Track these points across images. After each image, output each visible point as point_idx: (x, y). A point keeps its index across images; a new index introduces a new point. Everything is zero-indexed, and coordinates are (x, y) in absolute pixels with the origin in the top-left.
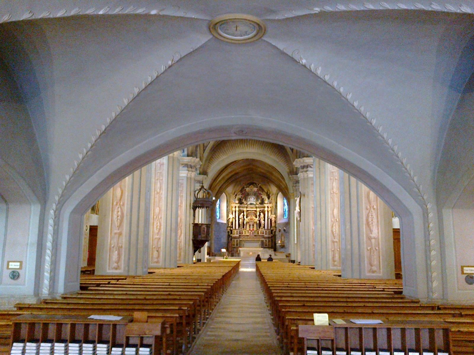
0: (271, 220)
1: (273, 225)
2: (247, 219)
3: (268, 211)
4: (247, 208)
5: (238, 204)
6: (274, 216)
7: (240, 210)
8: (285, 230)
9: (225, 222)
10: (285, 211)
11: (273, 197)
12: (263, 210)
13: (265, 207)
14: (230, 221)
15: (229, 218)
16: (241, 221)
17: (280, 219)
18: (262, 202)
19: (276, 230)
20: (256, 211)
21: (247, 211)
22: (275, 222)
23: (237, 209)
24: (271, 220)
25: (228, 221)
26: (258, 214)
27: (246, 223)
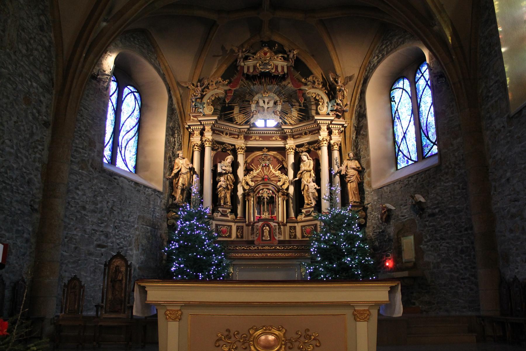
0: (343, 178)
1: (352, 198)
2: (248, 178)
3: (330, 148)
5: (214, 114)
6: (354, 164)
7: (222, 143)
8: (419, 208)
9: (160, 188)
10: (399, 140)
11: (346, 96)
12: (309, 143)
13: (318, 130)
14: (180, 184)
16: (222, 182)
17: (382, 173)
18: (306, 114)
19: (366, 218)
20: (282, 150)
21: (249, 150)
23: (208, 135)
24: (343, 178)
25: (171, 183)
26: (291, 159)
27: (244, 195)
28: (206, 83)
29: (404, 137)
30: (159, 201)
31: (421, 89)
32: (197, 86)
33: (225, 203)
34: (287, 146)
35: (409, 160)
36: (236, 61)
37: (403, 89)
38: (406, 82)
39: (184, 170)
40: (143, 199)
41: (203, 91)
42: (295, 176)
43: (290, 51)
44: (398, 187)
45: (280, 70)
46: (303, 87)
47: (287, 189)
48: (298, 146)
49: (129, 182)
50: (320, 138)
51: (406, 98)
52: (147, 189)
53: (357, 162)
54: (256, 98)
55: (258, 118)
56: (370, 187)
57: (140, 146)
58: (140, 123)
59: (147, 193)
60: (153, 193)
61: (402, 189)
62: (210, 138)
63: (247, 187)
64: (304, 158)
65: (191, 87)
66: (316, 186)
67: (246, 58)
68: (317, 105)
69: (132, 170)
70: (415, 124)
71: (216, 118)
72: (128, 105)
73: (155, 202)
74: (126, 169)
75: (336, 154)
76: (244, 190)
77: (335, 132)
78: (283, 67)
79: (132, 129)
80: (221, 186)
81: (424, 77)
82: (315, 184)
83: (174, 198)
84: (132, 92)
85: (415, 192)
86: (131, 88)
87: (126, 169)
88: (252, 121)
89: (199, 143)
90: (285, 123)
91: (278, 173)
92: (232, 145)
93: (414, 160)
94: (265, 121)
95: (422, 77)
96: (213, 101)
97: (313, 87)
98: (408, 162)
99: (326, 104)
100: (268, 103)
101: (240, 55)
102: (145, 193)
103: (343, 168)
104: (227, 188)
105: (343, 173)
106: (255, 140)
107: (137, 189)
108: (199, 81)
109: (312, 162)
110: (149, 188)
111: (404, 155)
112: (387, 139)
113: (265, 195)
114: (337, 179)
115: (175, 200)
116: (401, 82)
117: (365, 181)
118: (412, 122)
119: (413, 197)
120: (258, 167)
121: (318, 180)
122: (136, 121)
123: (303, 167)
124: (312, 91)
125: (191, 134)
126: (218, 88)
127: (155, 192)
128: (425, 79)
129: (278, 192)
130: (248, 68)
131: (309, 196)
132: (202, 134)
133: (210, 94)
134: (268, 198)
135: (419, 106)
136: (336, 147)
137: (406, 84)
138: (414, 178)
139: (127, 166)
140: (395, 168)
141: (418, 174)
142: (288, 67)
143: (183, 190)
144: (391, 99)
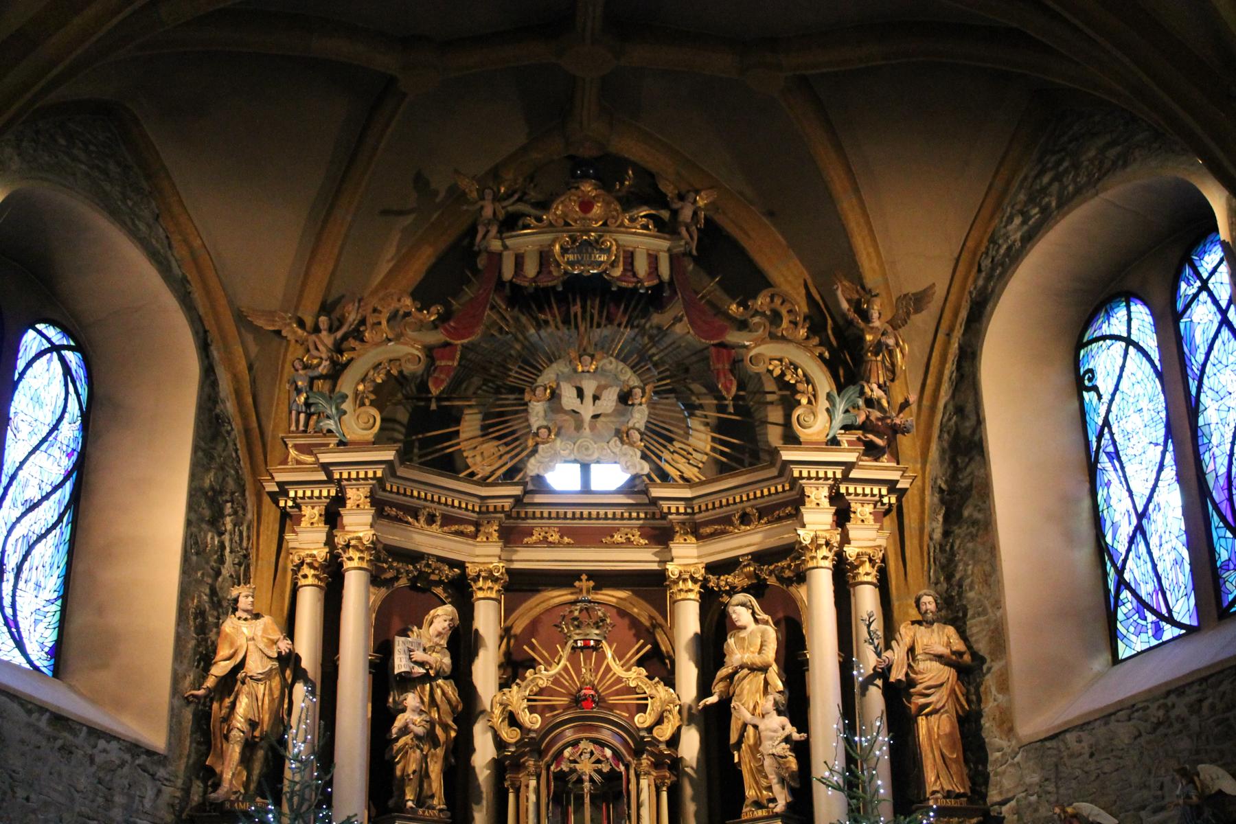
2: (516, 697)
4: (511, 536)
5: (379, 441)
6: (941, 639)
7: (415, 557)
9: (157, 739)
10: (1118, 540)
11: (904, 372)
12: (760, 557)
13: (794, 505)
14: (239, 721)
15: (220, 668)
16: (412, 712)
17: (1056, 677)
18: (746, 440)
20: (652, 585)
21: (520, 585)
22: (969, 727)
23: (358, 523)
25: (202, 718)
26: (688, 620)
27: (500, 767)
28: (352, 317)
29: (1140, 529)
30: (150, 793)
31: (1200, 339)
32: (316, 330)
33: (421, 801)
34: (673, 569)
35: (1163, 624)
36: (472, 231)
37: (1129, 341)
38: (1140, 312)
39: (256, 666)
40: (83, 783)
41: (338, 348)
42: (704, 689)
43: (681, 197)
44: (1123, 732)
45: (642, 267)
46: (733, 337)
47: (674, 741)
48: (715, 568)
49: (29, 712)
50: (805, 535)
51: (1139, 376)
52: (102, 744)
53: (950, 630)
54: (548, 377)
55: (555, 457)
56: (1010, 731)
57: (79, 567)
58: (82, 473)
59: (100, 759)
60: (127, 757)
61: (1142, 740)
62: (366, 534)
63: (510, 735)
64: (741, 615)
65: (292, 332)
66: (790, 729)
67: (510, 223)
68: (790, 404)
69: (42, 662)
70: (1180, 478)
71: (389, 455)
72: (37, 400)
73: (131, 798)
74: (19, 660)
75: (867, 600)
76: (500, 744)
77: (863, 511)
78: (653, 259)
79: (46, 497)
80: (405, 730)
81: (1211, 295)
82: (784, 720)
83: (211, 777)
84: (55, 348)
85: (1198, 756)
86: (53, 333)
87: (19, 660)
88: (532, 467)
89: (321, 553)
90: (664, 477)
91: (635, 676)
92: (452, 564)
93: (1186, 621)
94: (585, 468)
95: (1204, 296)
96: (377, 389)
97: (773, 337)
98: (1158, 631)
99: (823, 403)
100: (596, 398)
101: (488, 212)
102: (92, 761)
103: (897, 654)
104: (430, 738)
105: (897, 674)
106: (545, 543)
107: (59, 743)
108: (326, 308)
109: (771, 633)
110: (110, 737)
111: (1142, 604)
112: (1070, 538)
113: (586, 767)
114: (875, 699)
115: (217, 785)
116: (1121, 313)
117: (989, 707)
118: (1170, 473)
119: (1189, 776)
120: (554, 653)
121: (796, 706)
122: (67, 463)
123: (737, 653)
124: (769, 350)
125: (287, 520)
126: (398, 338)
127: (135, 756)
128: (1215, 302)
129: (637, 753)
130: (519, 260)
131: (760, 769)
132: (332, 517)
133: (365, 363)
134: (597, 777)
135: (1194, 408)
136: (867, 573)
137: (1138, 320)
138: (1191, 697)
139: (20, 645)
140: (1106, 657)
141: (1205, 679)
142: (674, 259)
143: (249, 746)
144: (1081, 382)
